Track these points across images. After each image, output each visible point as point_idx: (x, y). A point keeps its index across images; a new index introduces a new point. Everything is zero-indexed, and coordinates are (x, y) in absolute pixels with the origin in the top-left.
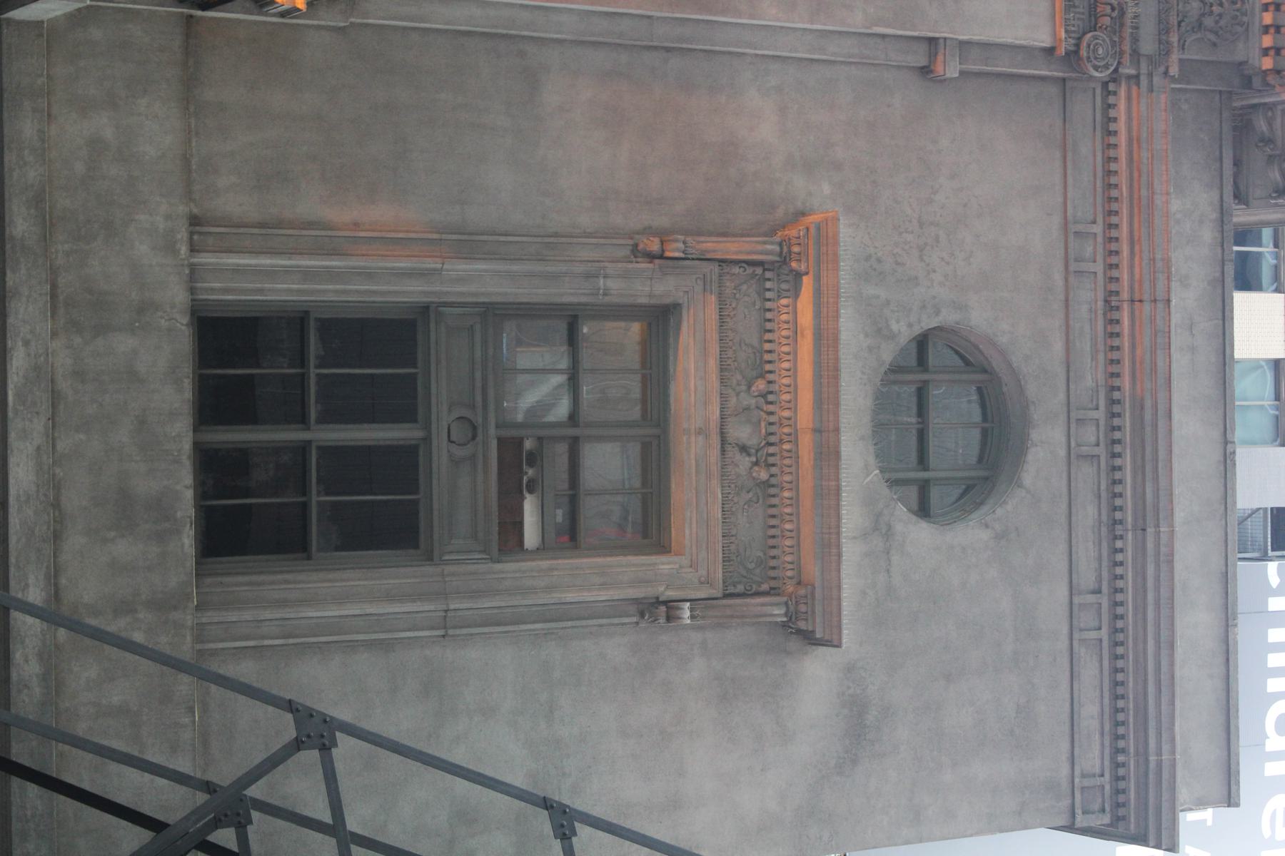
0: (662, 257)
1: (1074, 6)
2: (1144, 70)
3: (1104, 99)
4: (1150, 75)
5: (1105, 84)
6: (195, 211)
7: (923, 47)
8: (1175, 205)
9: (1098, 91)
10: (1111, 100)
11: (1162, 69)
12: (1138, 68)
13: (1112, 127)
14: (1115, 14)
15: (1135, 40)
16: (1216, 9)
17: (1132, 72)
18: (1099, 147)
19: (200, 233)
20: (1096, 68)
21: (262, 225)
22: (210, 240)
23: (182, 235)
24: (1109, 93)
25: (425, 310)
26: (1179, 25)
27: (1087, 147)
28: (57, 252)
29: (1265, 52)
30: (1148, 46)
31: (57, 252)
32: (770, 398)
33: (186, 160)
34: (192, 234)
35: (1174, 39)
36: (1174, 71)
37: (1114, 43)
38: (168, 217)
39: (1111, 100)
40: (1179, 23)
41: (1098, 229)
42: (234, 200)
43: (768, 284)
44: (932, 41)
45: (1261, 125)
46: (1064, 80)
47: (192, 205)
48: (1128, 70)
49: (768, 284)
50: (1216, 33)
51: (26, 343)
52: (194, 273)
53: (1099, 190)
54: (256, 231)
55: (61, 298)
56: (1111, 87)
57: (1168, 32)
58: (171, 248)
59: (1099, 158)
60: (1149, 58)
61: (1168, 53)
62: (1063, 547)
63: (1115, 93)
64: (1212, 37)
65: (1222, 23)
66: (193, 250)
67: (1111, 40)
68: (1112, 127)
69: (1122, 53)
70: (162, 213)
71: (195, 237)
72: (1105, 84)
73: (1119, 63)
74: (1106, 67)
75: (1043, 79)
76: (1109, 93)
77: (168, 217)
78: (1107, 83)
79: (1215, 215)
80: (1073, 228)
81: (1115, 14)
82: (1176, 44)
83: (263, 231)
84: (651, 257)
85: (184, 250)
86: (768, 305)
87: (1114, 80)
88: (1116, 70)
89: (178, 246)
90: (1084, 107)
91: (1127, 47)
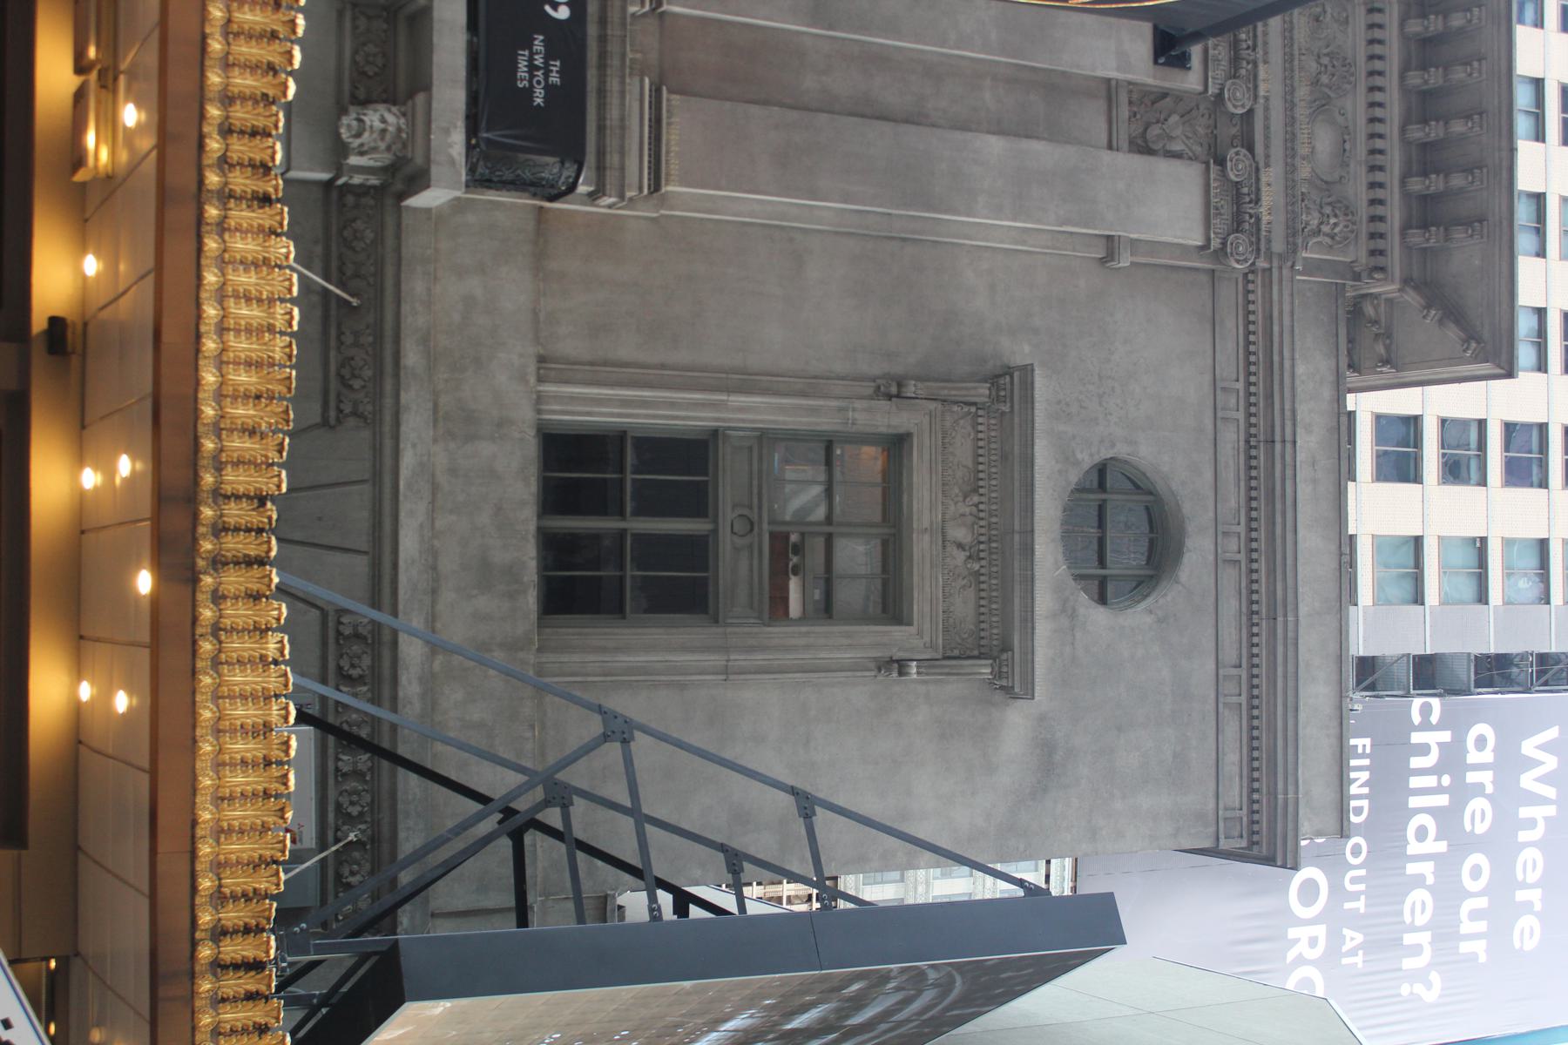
2: (1275, 264)
3: (1245, 287)
4: (1280, 268)
5: (1246, 275)
7: (1104, 241)
8: (1300, 369)
15: (1269, 241)
16: (1333, 221)
17: (1266, 265)
20: (1238, 261)
21: (592, 364)
22: (553, 373)
23: (532, 368)
25: (715, 433)
27: (1231, 326)
30: (1278, 246)
33: (535, 313)
35: (1300, 241)
37: (1251, 243)
38: (521, 355)
41: (1240, 385)
42: (571, 345)
44: (1109, 238)
45: (1369, 310)
48: (1262, 264)
51: (414, 446)
52: (540, 398)
53: (1241, 356)
56: (1251, 277)
57: (1294, 235)
58: (523, 378)
60: (1280, 255)
61: (1295, 252)
62: (1212, 631)
64: (1328, 240)
65: (1337, 230)
66: (540, 380)
69: (1258, 250)
70: (517, 353)
72: (1246, 275)
74: (1246, 260)
75: (1196, 269)
77: (521, 355)
79: (1331, 378)
80: (1220, 384)
85: (532, 380)
88: (1253, 264)
90: (1228, 294)
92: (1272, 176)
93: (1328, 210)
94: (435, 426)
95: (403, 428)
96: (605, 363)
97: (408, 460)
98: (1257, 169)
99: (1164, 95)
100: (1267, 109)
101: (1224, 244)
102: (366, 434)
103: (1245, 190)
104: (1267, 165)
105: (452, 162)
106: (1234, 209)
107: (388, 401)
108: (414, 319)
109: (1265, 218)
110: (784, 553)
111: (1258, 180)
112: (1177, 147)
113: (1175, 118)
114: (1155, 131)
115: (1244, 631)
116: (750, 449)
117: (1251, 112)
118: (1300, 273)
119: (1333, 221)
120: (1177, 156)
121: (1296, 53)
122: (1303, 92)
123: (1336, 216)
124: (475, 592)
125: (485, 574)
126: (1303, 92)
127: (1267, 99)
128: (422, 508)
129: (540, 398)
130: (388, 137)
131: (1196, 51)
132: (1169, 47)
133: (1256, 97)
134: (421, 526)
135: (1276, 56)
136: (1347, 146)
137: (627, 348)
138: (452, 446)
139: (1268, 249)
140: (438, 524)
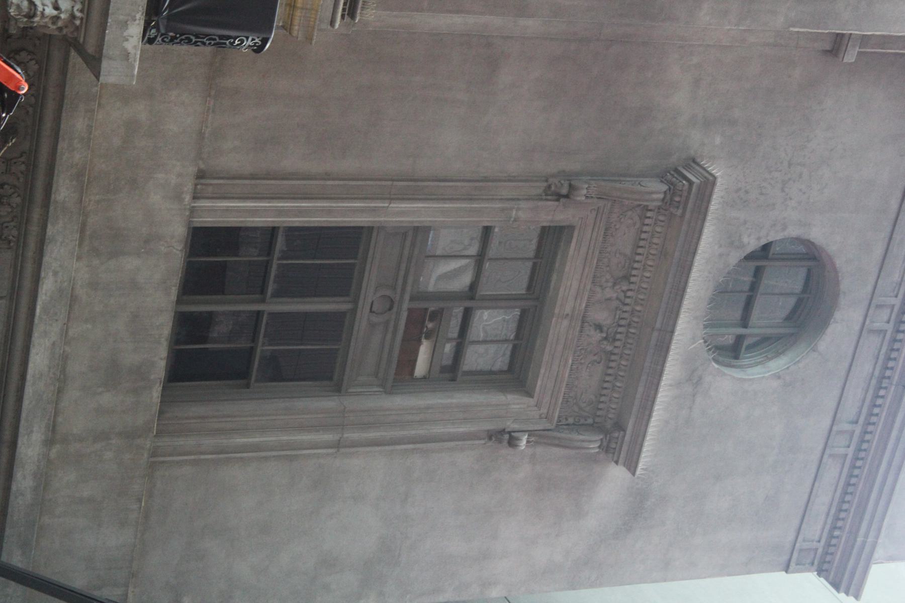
6: (202, 166)
19: (202, 184)
21: (253, 177)
22: (210, 189)
23: (189, 187)
25: (370, 229)
28: (90, 201)
31: (90, 201)
32: (629, 294)
33: (201, 135)
34: (196, 185)
38: (180, 175)
42: (233, 157)
47: (200, 162)
51: (55, 273)
52: (193, 210)
54: (247, 182)
55: (88, 233)
58: (178, 198)
62: (836, 392)
66: (195, 198)
70: (177, 172)
71: (199, 187)
77: (180, 175)
83: (253, 182)
85: (187, 198)
89: (184, 196)
94: (80, 245)
95: (46, 259)
96: (268, 176)
97: (47, 286)
102: (8, 256)
105: (126, 55)
107: (34, 229)
108: (71, 155)
110: (422, 320)
115: (871, 392)
116: (405, 235)
124: (100, 390)
125: (112, 374)
128: (55, 330)
129: (193, 210)
130: (60, 24)
134: (54, 344)
137: (293, 160)
138: (96, 262)
140: (71, 333)
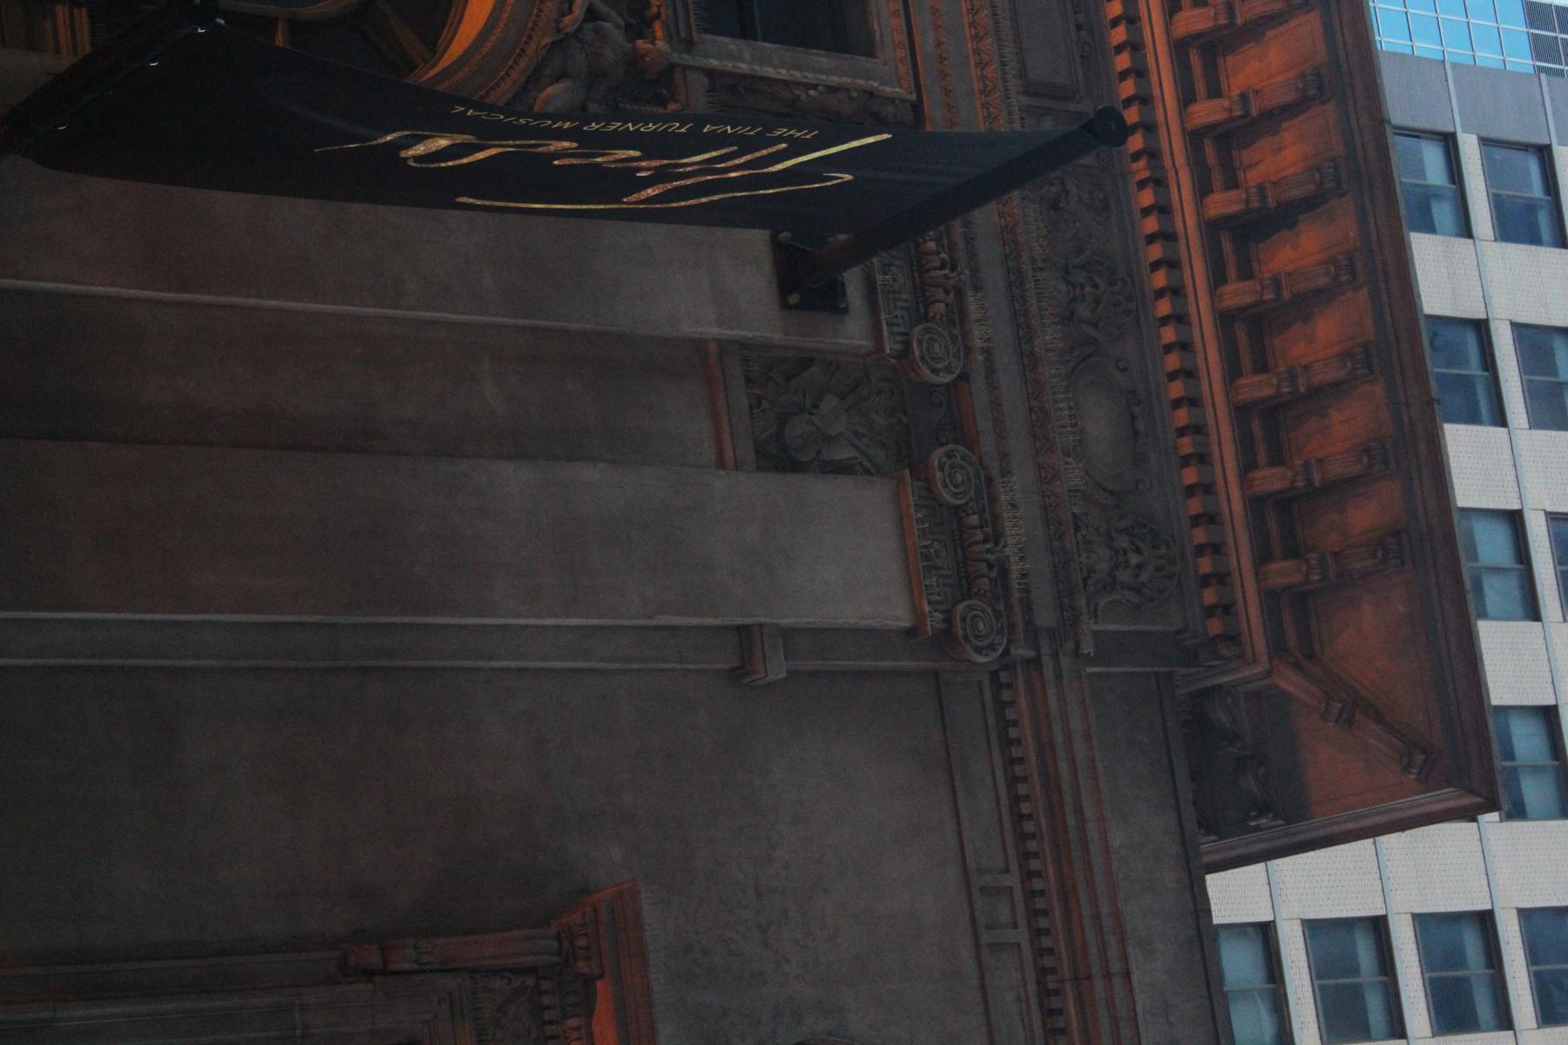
0: (385, 972)
1: (937, 568)
2: (1045, 649)
4: (1055, 656)
5: (994, 675)
8: (1116, 840)
9: (986, 683)
10: (1006, 695)
11: (1070, 646)
12: (1037, 647)
13: (1013, 733)
14: (994, 574)
15: (1028, 607)
16: (1134, 560)
17: (1031, 653)
18: (998, 761)
24: (1002, 686)
26: (1085, 584)
29: (1210, 611)
30: (1045, 617)
36: (1088, 648)
39: (1006, 695)
40: (1085, 580)
43: (547, 1000)
46: (936, 673)
48: (1022, 652)
49: (547, 1000)
50: (1138, 591)
56: (1004, 677)
59: (1001, 780)
63: (1009, 686)
64: (1131, 596)
67: (994, 610)
68: (1013, 733)
69: (1012, 627)
73: (1010, 642)
76: (1002, 686)
78: (996, 672)
81: (994, 574)
82: (1085, 610)
84: (368, 974)
86: (549, 1030)
87: (1005, 667)
88: (1006, 652)
91: (1018, 619)
92: (1018, 491)
93: (1123, 542)
98: (990, 481)
99: (806, 363)
100: (990, 371)
101: (949, 621)
103: (974, 520)
104: (1005, 472)
106: (956, 548)
109: (1015, 569)
111: (993, 499)
112: (843, 454)
113: (830, 403)
114: (798, 429)
117: (964, 377)
118: (1091, 661)
119: (1134, 560)
120: (843, 469)
121: (1027, 268)
122: (1049, 336)
123: (1138, 551)
126: (1049, 336)
127: (988, 353)
131: (853, 283)
132: (805, 282)
133: (968, 351)
135: (994, 277)
136: (1141, 426)
139: (1029, 623)
